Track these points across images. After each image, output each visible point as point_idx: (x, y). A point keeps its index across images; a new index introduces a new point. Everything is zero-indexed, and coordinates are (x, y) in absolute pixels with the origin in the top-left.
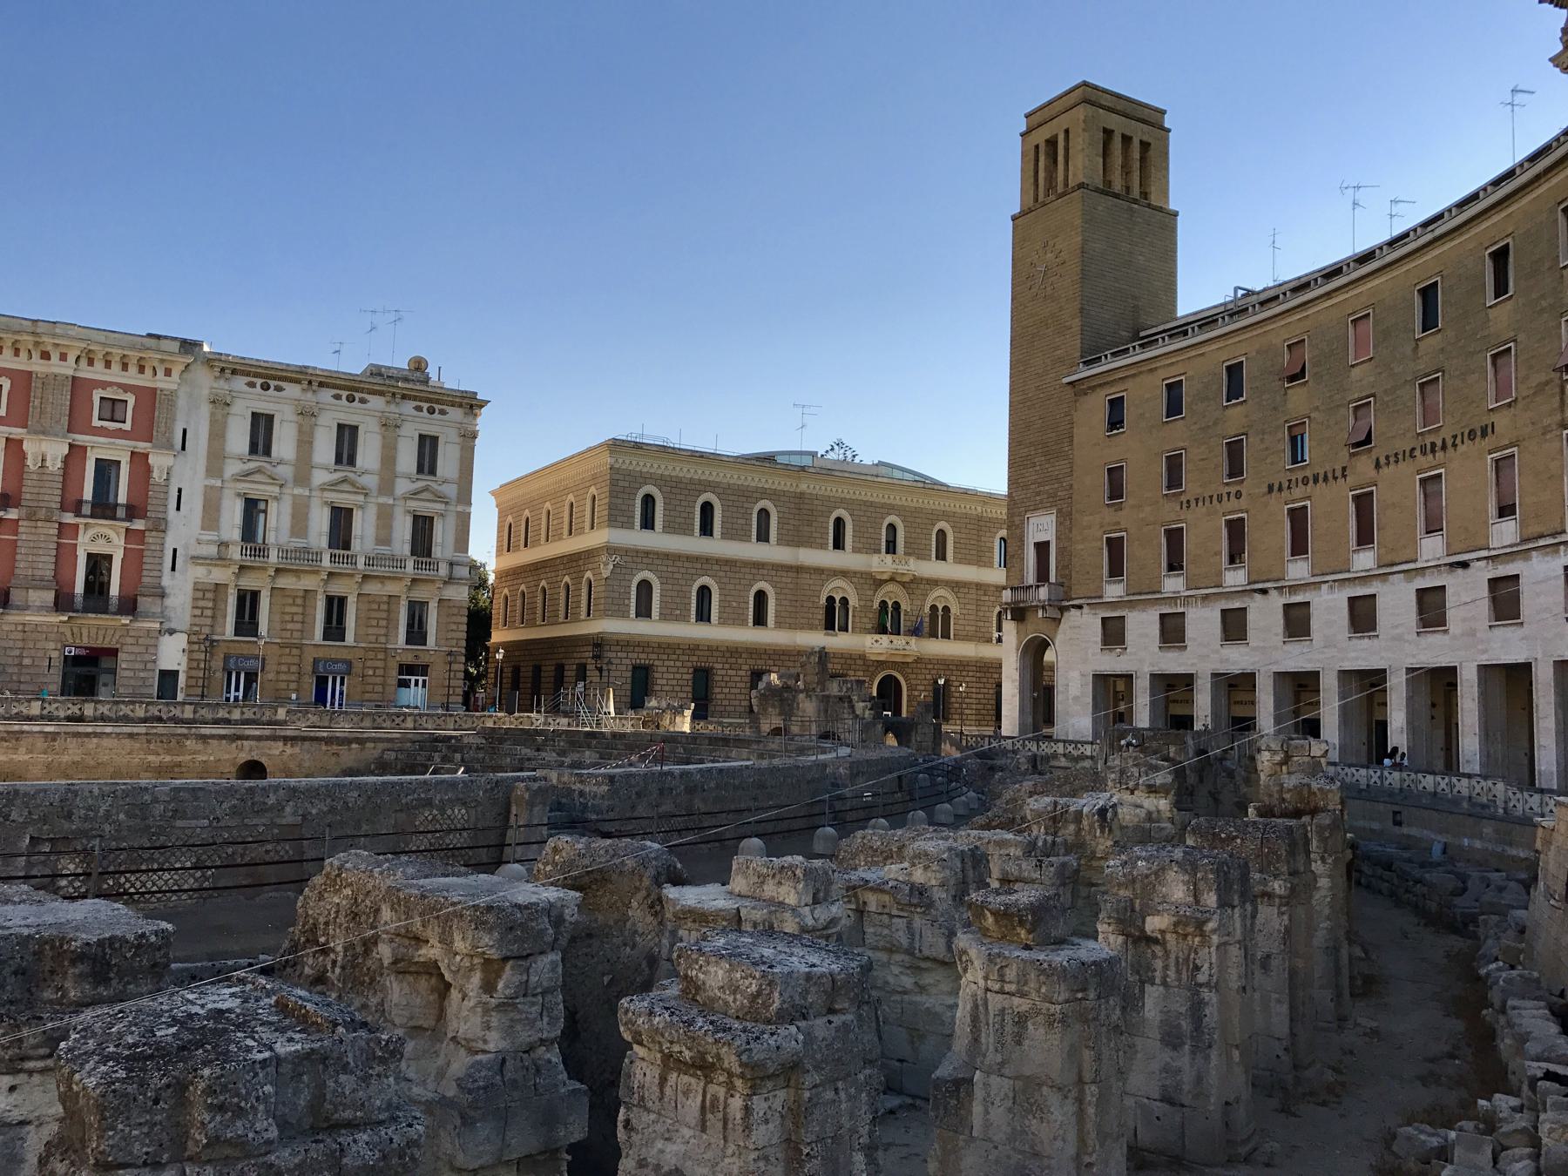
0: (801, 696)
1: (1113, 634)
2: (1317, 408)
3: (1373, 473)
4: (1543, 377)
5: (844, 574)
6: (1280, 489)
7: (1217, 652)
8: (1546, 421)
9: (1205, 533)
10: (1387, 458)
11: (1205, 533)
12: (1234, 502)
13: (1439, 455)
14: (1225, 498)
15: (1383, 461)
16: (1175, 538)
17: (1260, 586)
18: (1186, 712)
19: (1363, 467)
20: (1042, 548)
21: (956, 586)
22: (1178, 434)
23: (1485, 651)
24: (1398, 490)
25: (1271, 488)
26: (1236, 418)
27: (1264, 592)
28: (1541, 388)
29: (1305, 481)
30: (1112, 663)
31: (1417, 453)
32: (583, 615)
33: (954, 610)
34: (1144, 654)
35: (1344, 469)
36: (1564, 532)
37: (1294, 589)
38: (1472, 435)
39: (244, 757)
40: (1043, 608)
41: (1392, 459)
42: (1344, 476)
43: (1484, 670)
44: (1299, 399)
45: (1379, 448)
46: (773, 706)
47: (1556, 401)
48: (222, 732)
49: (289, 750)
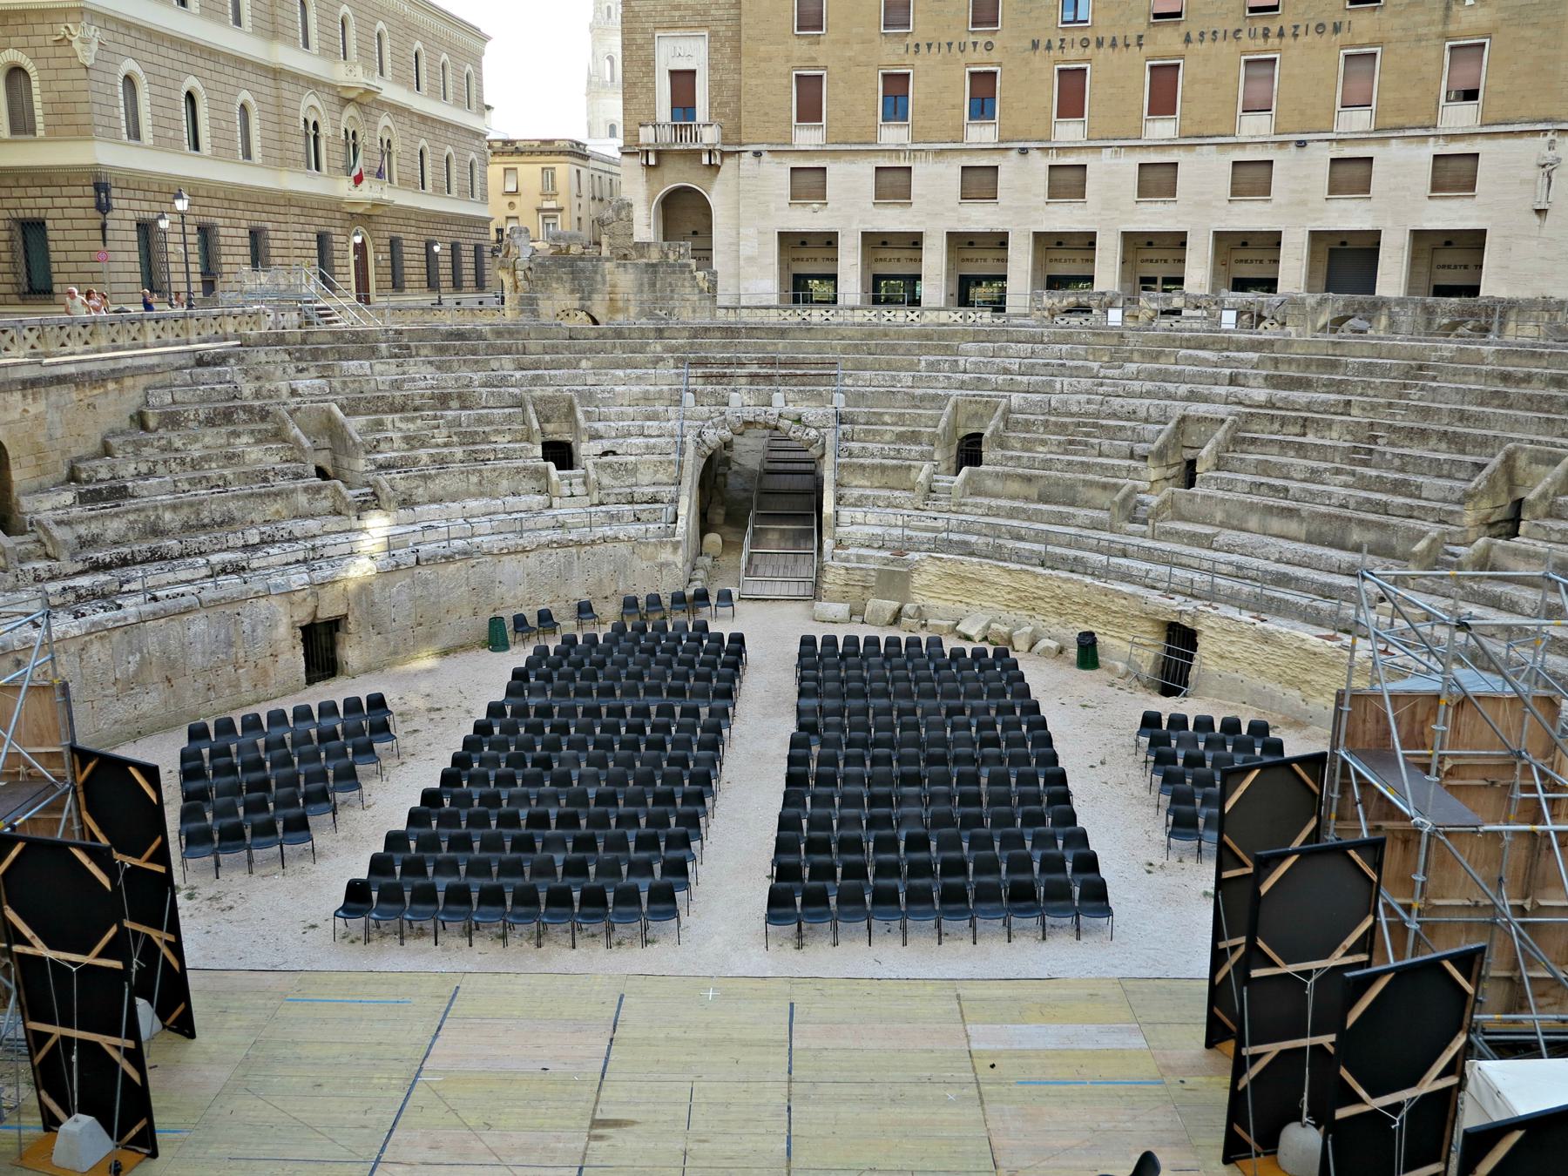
0: (608, 265)
1: (809, 183)
3: (1179, 47)
5: (314, 84)
6: (1049, 47)
7: (953, 210)
8: (1421, 31)
10: (1202, 34)
11: (939, 84)
12: (980, 54)
13: (1274, 41)
14: (970, 47)
15: (1195, 35)
16: (896, 86)
17: (1022, 145)
19: (1167, 41)
21: (398, 110)
24: (1210, 71)
25: (1035, 45)
27: (1024, 151)
29: (1085, 43)
30: (806, 220)
31: (1244, 35)
34: (850, 208)
35: (1140, 37)
36: (1435, 127)
37: (1062, 150)
38: (1320, 28)
40: (710, 152)
41: (1208, 36)
42: (1140, 45)
43: (1315, 236)
45: (1190, 24)
46: (559, 279)
47: (1438, 15)
49: (33, 409)
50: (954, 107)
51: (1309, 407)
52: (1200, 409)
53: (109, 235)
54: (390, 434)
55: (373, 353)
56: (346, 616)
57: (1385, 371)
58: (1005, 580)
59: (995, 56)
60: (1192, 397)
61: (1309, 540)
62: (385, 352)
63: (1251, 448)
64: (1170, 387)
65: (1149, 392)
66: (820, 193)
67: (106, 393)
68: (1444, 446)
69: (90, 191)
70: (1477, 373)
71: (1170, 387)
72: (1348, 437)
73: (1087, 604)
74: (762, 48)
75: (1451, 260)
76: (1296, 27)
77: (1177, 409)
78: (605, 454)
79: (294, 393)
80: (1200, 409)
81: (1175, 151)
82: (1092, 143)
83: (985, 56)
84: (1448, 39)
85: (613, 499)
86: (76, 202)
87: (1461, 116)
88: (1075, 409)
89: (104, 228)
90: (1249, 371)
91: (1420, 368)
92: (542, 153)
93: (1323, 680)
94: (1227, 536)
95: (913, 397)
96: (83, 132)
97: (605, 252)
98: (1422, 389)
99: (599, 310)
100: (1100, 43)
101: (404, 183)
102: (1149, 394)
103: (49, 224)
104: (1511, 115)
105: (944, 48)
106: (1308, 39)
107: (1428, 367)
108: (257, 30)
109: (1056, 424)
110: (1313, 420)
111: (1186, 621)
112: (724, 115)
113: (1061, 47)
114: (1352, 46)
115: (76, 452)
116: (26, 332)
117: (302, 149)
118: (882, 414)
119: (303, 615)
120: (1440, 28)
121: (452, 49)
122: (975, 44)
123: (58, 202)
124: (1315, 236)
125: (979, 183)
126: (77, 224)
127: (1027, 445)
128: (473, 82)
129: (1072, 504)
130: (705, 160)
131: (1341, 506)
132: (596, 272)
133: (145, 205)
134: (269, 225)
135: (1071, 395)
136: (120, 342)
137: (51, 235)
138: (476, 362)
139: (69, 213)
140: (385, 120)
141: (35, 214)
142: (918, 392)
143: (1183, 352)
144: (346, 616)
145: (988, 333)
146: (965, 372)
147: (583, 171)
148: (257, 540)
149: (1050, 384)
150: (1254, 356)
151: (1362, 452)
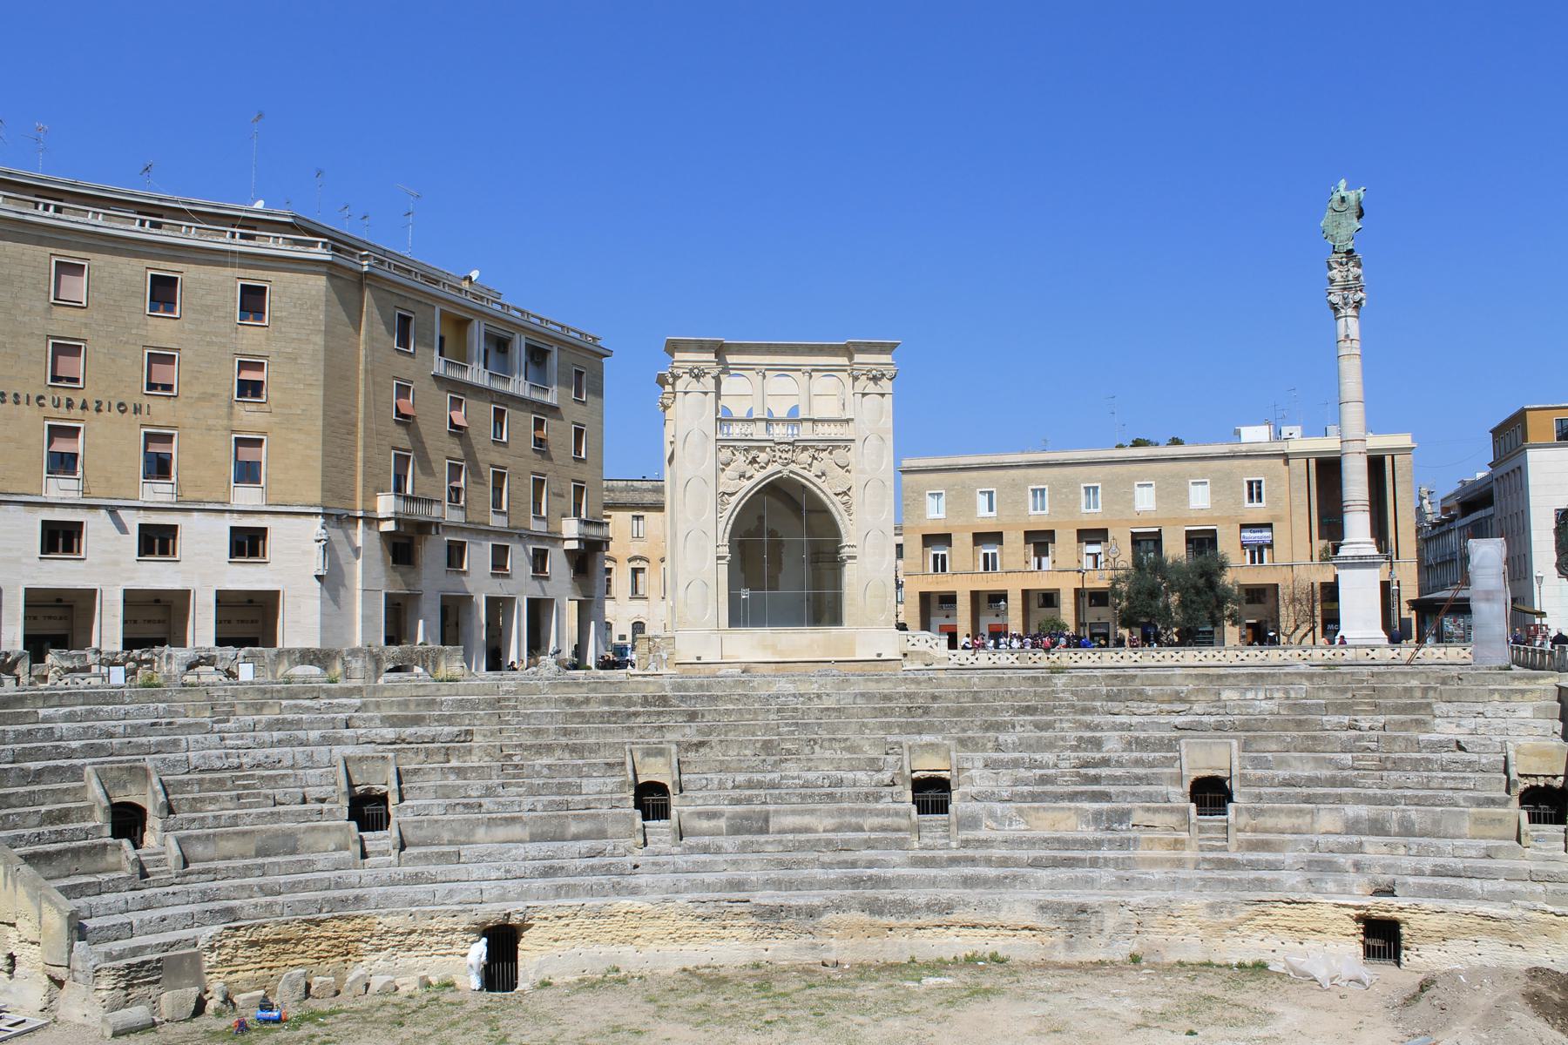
4: (210, 390)
23: (130, 579)
31: (48, 402)
57: (475, 706)
60: (325, 741)
61: (534, 838)
65: (279, 742)
68: (567, 755)
70: (548, 701)
75: (248, 619)
84: (233, 431)
87: (246, 497)
88: (218, 764)
93: (652, 931)
94: (465, 851)
98: (518, 715)
102: (280, 743)
104: (288, 499)
109: (211, 780)
120: (225, 422)
124: (128, 593)
127: (195, 804)
129: (293, 852)
143: (284, 703)
149: (175, 743)
150: (357, 701)
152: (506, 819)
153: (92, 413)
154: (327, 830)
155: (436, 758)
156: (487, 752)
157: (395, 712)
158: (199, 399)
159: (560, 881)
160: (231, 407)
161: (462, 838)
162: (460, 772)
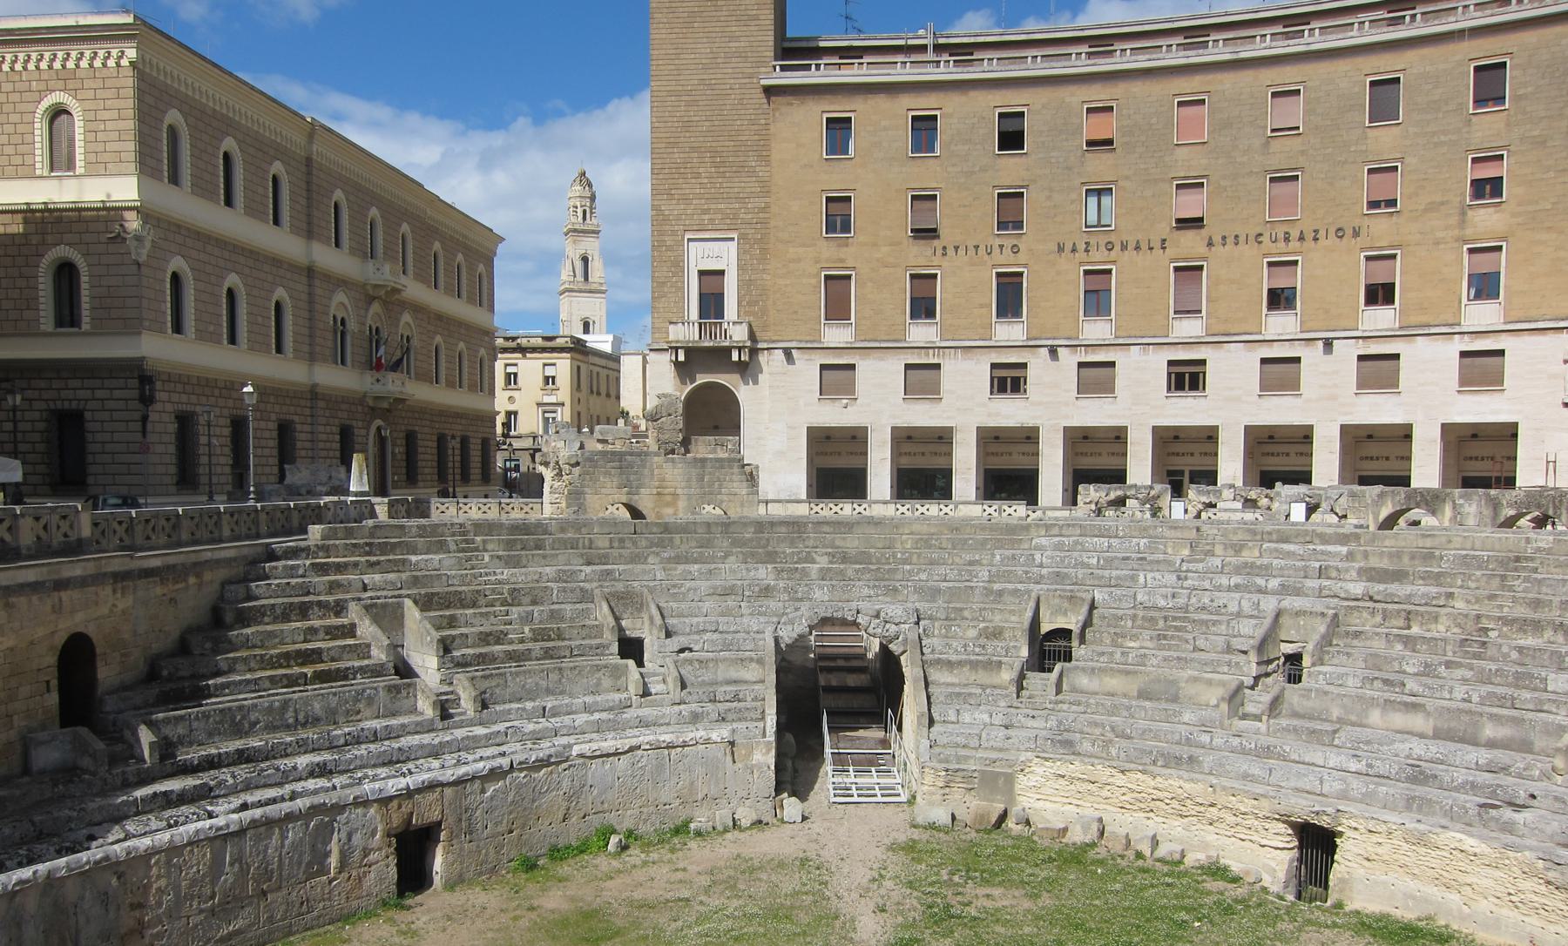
1: (837, 378)
2: (1127, 178)
3: (1202, 249)
4: (1438, 199)
5: (343, 283)
6: (1074, 250)
8: (1440, 234)
9: (965, 283)
10: (1224, 238)
13: (1294, 245)
14: (996, 250)
15: (1217, 239)
17: (1050, 342)
18: (938, 463)
19: (1190, 245)
20: (711, 277)
21: (418, 309)
22: (926, 174)
25: (1061, 249)
26: (1011, 170)
28: (1432, 208)
29: (1110, 247)
30: (835, 415)
31: (1265, 239)
32: (47, 320)
33: (415, 342)
34: (880, 406)
39: (66, 627)
40: (740, 349)
41: (1230, 240)
44: (1100, 166)
45: (1212, 228)
46: (607, 474)
47: (1454, 220)
48: (30, 576)
50: (981, 306)
51: (1408, 599)
52: (1290, 602)
53: (149, 427)
54: (464, 630)
55: (441, 547)
56: (439, 823)
58: (1120, 779)
59: (1022, 257)
60: (1284, 590)
61: (1438, 735)
62: (453, 547)
63: (1355, 642)
64: (1260, 581)
65: (1237, 586)
66: (848, 389)
67: (187, 588)
69: (135, 383)
71: (1260, 581)
72: (1456, 630)
73: (1212, 805)
74: (791, 250)
76: (1316, 231)
77: (1269, 604)
78: (682, 651)
79: (365, 588)
80: (1290, 602)
81: (1203, 348)
82: (1121, 341)
83: (1012, 258)
84: (1466, 242)
85: (695, 697)
86: (117, 394)
89: (145, 419)
90: (1340, 565)
91: (1517, 559)
92: (544, 350)
95: (992, 592)
96: (131, 327)
97: (654, 447)
98: (1526, 580)
99: (645, 503)
100: (1124, 247)
101: (422, 377)
103: (88, 415)
105: (972, 251)
106: (1328, 243)
107: (1527, 559)
108: (295, 230)
110: (1417, 612)
111: (1324, 821)
112: (754, 314)
113: (1087, 251)
114: (1372, 248)
115: (156, 647)
116: (115, 525)
117: (330, 344)
118: (961, 610)
119: (396, 820)
121: (468, 250)
122: (1001, 247)
123: (99, 394)
125: (1008, 381)
126: (116, 415)
128: (485, 283)
130: (735, 357)
131: (1464, 700)
132: (644, 467)
133: (184, 398)
134: (296, 418)
135: (1154, 588)
136: (198, 535)
137: (89, 426)
138: (544, 557)
139: (110, 404)
140: (406, 317)
141: (74, 405)
142: (996, 587)
144: (439, 823)
145: (1061, 527)
146: (1041, 566)
147: (583, 367)
148: (342, 741)
150: (1344, 550)
151: (1475, 641)
152: (1406, 704)
153: (1309, 243)
154: (1209, 682)
155: (1394, 622)
156: (1458, 620)
157: (1384, 564)
158: (1425, 211)
159: (1419, 790)
160: (1463, 214)
161: (1353, 718)
162: (1409, 642)
